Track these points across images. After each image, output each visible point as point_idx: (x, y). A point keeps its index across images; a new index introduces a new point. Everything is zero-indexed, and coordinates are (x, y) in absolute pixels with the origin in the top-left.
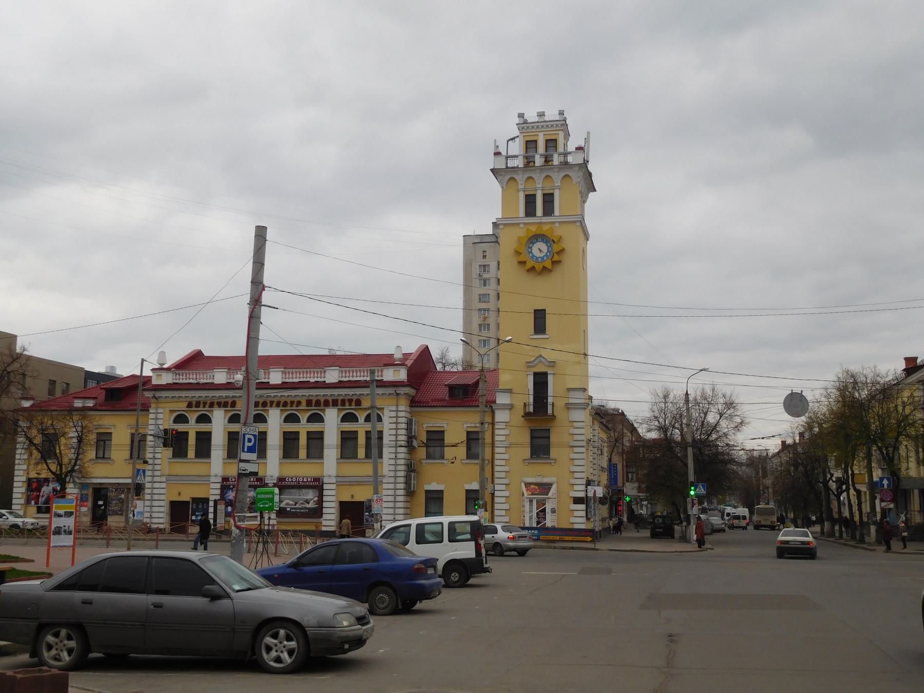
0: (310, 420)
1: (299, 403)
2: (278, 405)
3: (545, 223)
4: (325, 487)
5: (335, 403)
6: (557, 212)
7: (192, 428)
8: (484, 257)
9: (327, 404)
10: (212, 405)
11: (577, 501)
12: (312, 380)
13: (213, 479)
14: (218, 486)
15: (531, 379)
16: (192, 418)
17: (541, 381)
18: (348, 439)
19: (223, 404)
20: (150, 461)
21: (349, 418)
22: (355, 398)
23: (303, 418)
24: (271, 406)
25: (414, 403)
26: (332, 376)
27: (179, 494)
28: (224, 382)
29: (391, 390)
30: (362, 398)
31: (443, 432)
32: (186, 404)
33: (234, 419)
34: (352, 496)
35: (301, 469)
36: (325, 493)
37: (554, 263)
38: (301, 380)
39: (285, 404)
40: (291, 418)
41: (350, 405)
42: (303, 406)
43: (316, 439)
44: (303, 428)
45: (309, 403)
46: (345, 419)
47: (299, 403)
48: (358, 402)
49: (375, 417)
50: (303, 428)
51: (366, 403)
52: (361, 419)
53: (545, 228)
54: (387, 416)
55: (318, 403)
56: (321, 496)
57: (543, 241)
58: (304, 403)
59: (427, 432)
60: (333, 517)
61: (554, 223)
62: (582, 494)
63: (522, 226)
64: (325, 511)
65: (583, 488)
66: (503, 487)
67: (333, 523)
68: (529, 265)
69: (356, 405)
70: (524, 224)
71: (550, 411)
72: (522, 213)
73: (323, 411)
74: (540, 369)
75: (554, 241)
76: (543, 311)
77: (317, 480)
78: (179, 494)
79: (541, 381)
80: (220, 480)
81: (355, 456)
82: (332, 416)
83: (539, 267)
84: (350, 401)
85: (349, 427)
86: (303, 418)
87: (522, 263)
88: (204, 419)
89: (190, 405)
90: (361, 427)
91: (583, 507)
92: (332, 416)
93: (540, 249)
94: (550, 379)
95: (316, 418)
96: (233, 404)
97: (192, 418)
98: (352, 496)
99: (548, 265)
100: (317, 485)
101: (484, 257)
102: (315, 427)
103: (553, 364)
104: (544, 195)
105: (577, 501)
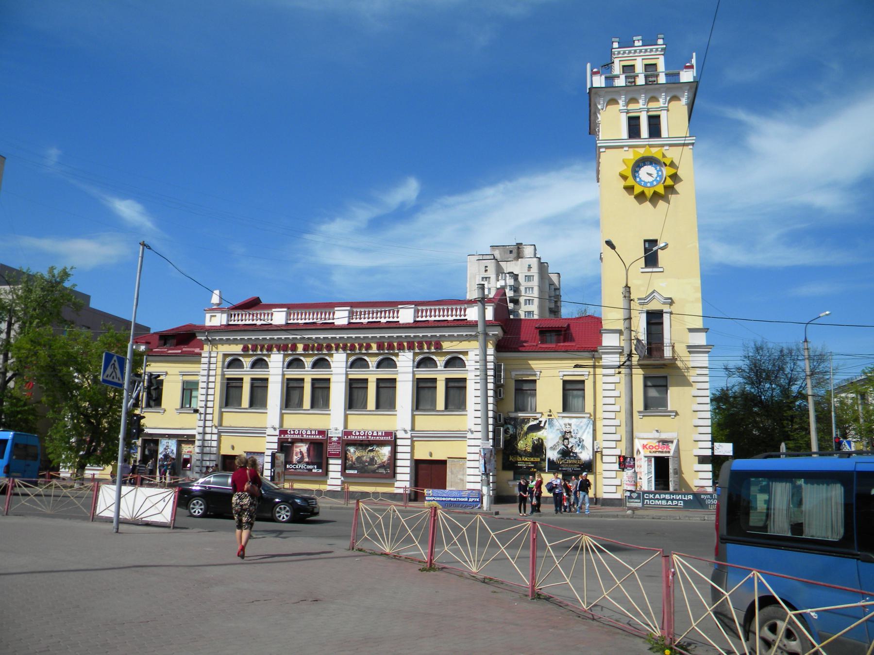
0: (379, 365)
2: (344, 348)
3: (651, 146)
4: (399, 442)
5: (411, 347)
6: (664, 133)
7: (247, 374)
8: (486, 271)
9: (401, 347)
10: (270, 349)
11: (703, 460)
12: (383, 320)
13: (270, 431)
14: (275, 439)
15: (644, 315)
16: (247, 362)
17: (655, 319)
19: (282, 348)
20: (202, 410)
21: (426, 362)
22: (434, 340)
23: (372, 362)
24: (337, 349)
25: (500, 347)
26: (406, 316)
27: (233, 448)
28: (284, 323)
31: (535, 381)
32: (241, 347)
33: (295, 363)
34: (431, 455)
35: (368, 423)
36: (399, 449)
37: (667, 188)
38: (371, 320)
40: (359, 363)
41: (429, 348)
42: (374, 349)
43: (387, 387)
44: (372, 375)
45: (380, 347)
46: (419, 364)
47: (369, 347)
48: (438, 346)
49: (455, 361)
50: (372, 375)
51: (447, 346)
53: (654, 152)
54: (472, 360)
56: (394, 452)
57: (651, 164)
59: (517, 381)
60: (407, 477)
61: (663, 146)
62: (708, 453)
63: (626, 149)
64: (399, 470)
65: (709, 444)
66: (613, 444)
67: (408, 484)
68: (638, 190)
69: (436, 348)
70: (630, 147)
71: (668, 353)
72: (624, 134)
73: (397, 355)
74: (654, 306)
75: (666, 165)
76: (654, 242)
77: (388, 434)
78: (233, 448)
79: (655, 319)
80: (277, 433)
81: (432, 407)
82: (405, 361)
83: (649, 193)
85: (425, 373)
86: (372, 362)
87: (629, 189)
88: (259, 363)
89: (245, 349)
90: (441, 375)
91: (709, 467)
92: (405, 361)
93: (647, 173)
94: (666, 318)
95: (387, 363)
96: (294, 348)
97: (247, 362)
98: (431, 455)
99: (661, 190)
100: (391, 440)
101: (486, 271)
102: (385, 374)
103: (671, 302)
104: (650, 118)
105: (703, 460)
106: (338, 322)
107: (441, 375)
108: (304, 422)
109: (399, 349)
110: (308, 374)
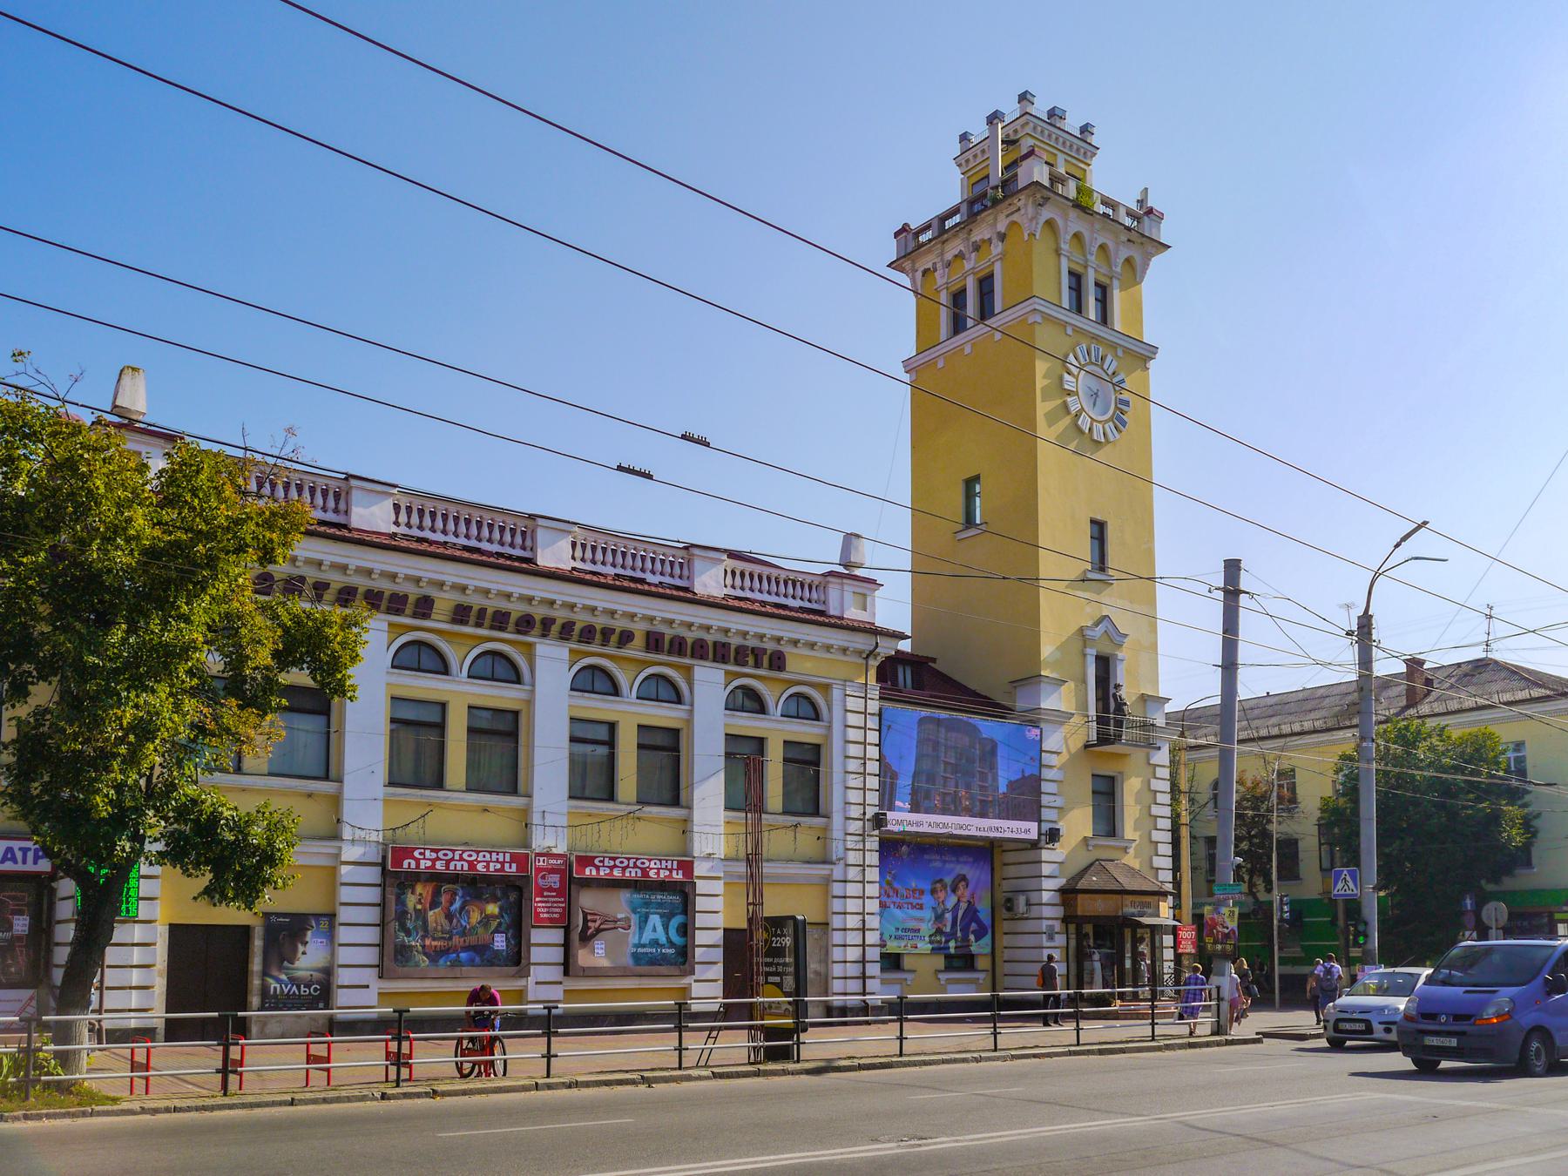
1: (626, 638)
9: (700, 650)
18: (744, 756)
29: (862, 642)
30: (787, 649)
39: (588, 634)
48: (778, 661)
51: (800, 664)
52: (775, 710)
55: (678, 646)
58: (639, 641)
72: (1066, 304)
84: (757, 654)
85: (748, 724)
90: (777, 730)
92: (710, 685)
102: (663, 715)
106: (545, 560)
107: (777, 730)
108: (462, 825)
109: (693, 656)
110: (461, 693)
